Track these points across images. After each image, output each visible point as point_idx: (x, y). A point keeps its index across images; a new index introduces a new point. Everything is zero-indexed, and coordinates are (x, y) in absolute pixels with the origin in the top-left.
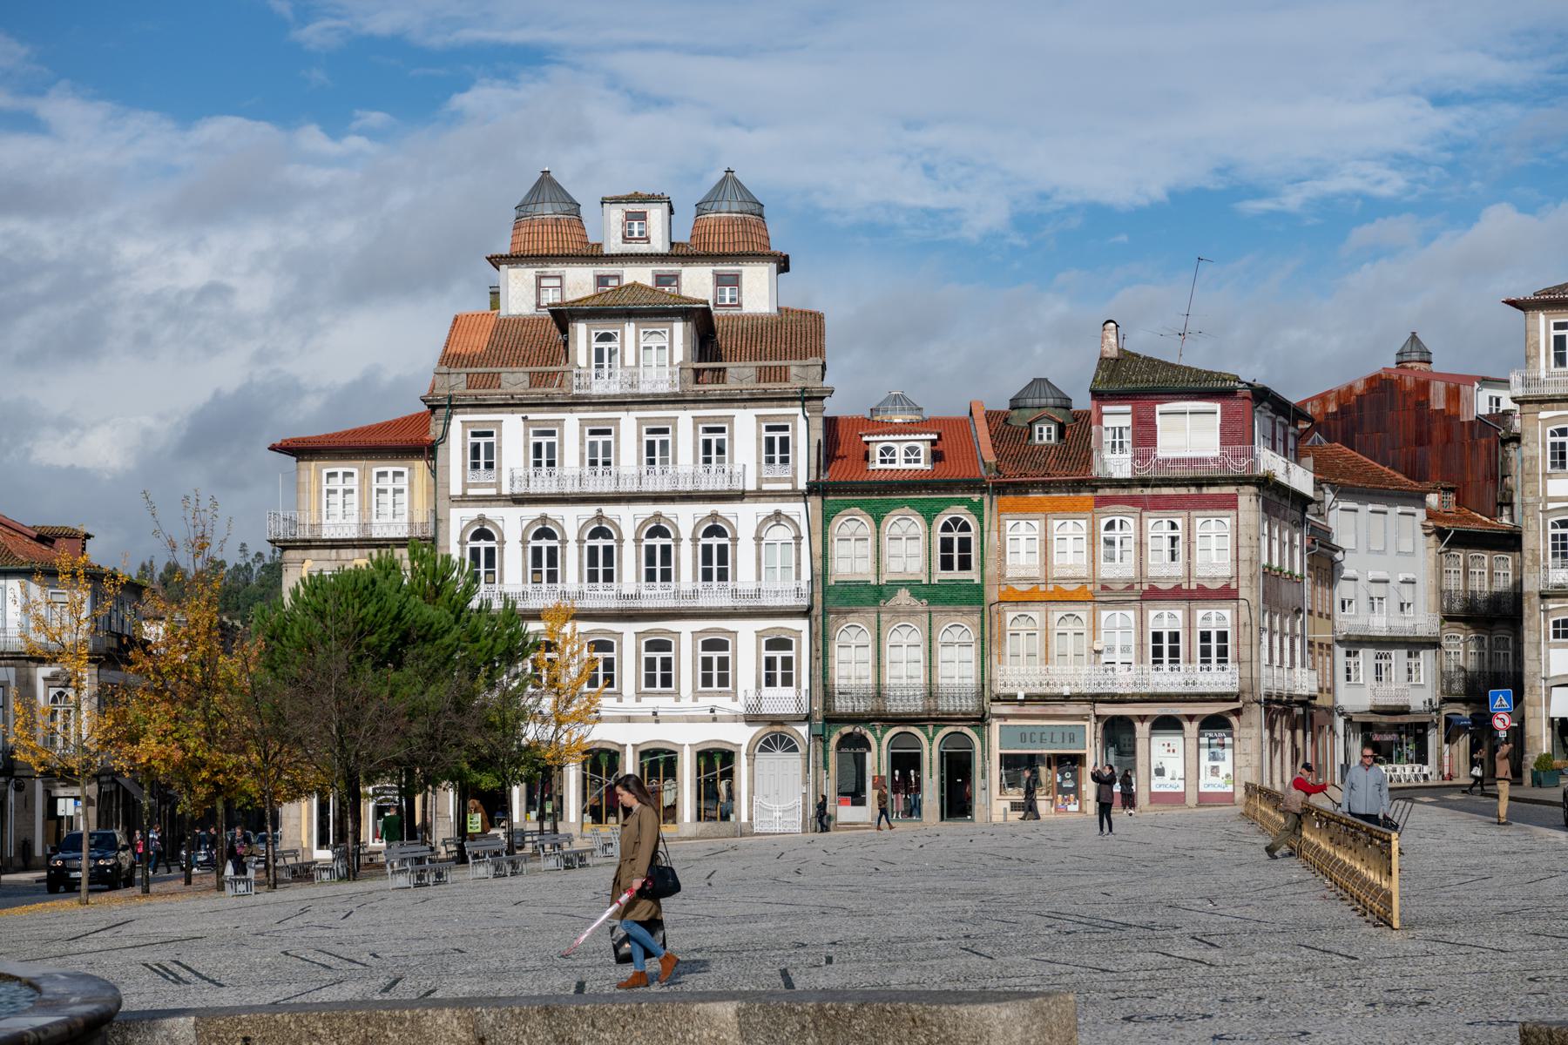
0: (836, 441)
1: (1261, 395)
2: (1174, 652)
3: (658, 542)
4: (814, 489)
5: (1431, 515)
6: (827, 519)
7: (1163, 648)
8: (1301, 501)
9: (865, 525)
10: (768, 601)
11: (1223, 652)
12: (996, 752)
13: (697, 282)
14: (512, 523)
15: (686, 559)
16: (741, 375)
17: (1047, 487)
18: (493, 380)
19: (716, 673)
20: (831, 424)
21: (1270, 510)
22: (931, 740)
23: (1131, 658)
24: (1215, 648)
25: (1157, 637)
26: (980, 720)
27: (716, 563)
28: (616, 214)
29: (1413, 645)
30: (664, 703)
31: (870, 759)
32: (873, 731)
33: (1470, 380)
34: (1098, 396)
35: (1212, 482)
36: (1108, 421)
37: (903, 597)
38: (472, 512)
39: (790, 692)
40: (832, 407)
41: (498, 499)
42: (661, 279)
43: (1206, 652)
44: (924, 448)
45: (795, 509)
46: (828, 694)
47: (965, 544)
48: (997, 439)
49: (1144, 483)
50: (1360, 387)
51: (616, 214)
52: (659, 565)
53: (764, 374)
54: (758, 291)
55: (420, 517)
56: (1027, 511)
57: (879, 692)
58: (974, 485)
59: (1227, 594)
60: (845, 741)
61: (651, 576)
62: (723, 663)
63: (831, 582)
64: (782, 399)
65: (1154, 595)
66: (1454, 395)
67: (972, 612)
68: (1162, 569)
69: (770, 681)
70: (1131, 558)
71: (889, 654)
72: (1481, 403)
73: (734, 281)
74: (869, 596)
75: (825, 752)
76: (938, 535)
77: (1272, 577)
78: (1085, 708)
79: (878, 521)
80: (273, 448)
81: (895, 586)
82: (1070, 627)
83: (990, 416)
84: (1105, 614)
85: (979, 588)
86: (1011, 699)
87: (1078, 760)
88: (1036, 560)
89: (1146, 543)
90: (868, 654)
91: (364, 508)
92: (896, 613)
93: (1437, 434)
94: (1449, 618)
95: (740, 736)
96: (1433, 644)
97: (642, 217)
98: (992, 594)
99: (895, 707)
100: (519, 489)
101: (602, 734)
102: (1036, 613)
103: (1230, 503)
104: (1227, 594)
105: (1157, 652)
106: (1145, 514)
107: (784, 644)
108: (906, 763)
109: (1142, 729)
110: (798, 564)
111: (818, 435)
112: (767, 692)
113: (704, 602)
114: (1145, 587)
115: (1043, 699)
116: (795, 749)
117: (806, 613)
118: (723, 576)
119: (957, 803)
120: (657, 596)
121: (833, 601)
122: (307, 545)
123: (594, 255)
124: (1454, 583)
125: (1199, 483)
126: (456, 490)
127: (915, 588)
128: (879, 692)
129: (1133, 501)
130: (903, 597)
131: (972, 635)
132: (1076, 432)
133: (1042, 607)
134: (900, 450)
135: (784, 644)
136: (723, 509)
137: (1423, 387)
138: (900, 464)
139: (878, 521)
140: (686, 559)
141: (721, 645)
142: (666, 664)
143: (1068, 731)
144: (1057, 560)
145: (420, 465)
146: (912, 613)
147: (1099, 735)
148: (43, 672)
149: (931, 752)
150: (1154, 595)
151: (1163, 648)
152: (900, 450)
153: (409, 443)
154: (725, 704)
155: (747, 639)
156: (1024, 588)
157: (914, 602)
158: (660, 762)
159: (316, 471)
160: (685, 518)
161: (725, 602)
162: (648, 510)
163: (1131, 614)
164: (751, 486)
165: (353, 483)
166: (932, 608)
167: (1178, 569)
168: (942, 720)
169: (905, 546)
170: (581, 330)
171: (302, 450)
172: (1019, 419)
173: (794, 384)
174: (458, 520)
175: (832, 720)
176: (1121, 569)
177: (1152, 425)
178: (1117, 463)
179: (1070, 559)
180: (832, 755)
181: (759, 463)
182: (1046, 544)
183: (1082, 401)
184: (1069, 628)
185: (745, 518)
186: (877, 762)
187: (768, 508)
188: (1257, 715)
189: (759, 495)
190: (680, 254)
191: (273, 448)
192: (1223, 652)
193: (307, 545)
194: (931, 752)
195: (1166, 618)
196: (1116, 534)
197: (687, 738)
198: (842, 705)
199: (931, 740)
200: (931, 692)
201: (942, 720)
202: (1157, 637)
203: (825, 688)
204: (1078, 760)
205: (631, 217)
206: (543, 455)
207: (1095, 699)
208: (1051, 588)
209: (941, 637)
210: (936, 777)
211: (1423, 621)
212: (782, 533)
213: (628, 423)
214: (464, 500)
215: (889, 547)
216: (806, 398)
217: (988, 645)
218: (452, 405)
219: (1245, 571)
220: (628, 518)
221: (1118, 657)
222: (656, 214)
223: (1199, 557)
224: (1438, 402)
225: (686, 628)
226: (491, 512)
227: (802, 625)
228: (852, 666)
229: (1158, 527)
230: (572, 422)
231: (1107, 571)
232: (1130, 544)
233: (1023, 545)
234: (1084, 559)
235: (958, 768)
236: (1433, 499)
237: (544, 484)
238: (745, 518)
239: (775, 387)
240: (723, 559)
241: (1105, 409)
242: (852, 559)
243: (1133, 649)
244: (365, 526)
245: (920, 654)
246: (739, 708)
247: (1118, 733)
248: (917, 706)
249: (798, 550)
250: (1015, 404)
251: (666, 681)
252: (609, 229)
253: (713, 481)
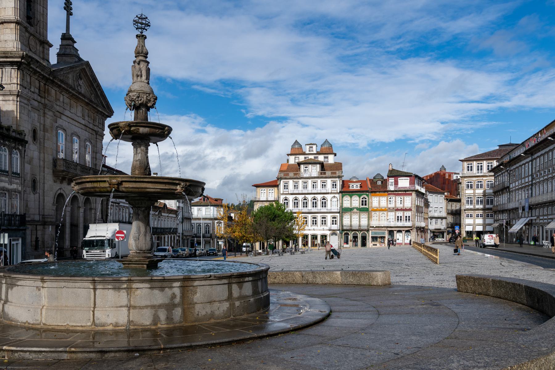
0: (344, 184)
1: (416, 176)
2: (401, 219)
3: (315, 201)
4: (340, 192)
5: (445, 196)
6: (342, 197)
7: (399, 219)
8: (423, 194)
9: (349, 198)
10: (332, 211)
11: (409, 219)
12: (370, 236)
13: (321, 158)
14: (291, 198)
15: (319, 203)
16: (328, 173)
17: (379, 192)
18: (288, 175)
19: (324, 222)
20: (343, 181)
21: (417, 196)
24: (408, 219)
25: (398, 217)
26: (368, 231)
27: (324, 204)
28: (308, 147)
29: (442, 218)
30: (315, 227)
31: (349, 237)
33: (452, 173)
34: (388, 176)
35: (408, 191)
36: (390, 181)
37: (355, 210)
38: (284, 196)
39: (336, 226)
40: (343, 179)
41: (288, 194)
42: (315, 158)
43: (406, 219)
44: (359, 185)
45: (337, 195)
46: (342, 226)
47: (366, 201)
48: (371, 184)
49: (396, 191)
50: (433, 175)
51: (308, 147)
52: (315, 205)
53: (332, 173)
54: (331, 159)
55: (276, 197)
56: (376, 196)
57: (351, 226)
58: (367, 191)
59: (410, 210)
60: (345, 234)
61: (313, 206)
62: (325, 221)
64: (335, 177)
65: (397, 210)
66: (450, 176)
68: (399, 206)
69: (333, 224)
70: (394, 204)
71: (353, 220)
72: (455, 177)
73: (327, 158)
74: (349, 210)
76: (361, 200)
77: (418, 207)
78: (385, 229)
79: (351, 197)
81: (354, 208)
82: (383, 215)
83: (370, 180)
85: (368, 209)
86: (373, 227)
87: (384, 237)
88: (378, 204)
89: (397, 201)
90: (349, 219)
91: (267, 195)
92: (354, 213)
93: (447, 183)
94: (448, 214)
95: (328, 233)
96: (446, 218)
97: (312, 147)
98: (370, 210)
99: (353, 228)
100: (292, 192)
101: (306, 232)
102: (377, 213)
103: (411, 194)
104: (410, 210)
105: (398, 219)
107: (335, 218)
108: (355, 237)
109: (395, 232)
111: (341, 183)
112: (332, 226)
113: (322, 211)
115: (378, 227)
117: (339, 213)
118: (325, 206)
119: (364, 244)
120: (314, 210)
121: (344, 211)
122: (258, 201)
123: (304, 154)
124: (449, 208)
125: (405, 191)
126: (282, 192)
127: (357, 209)
128: (351, 226)
130: (355, 210)
131: (367, 216)
132: (385, 183)
134: (355, 186)
135: (335, 218)
136: (325, 195)
137: (444, 174)
138: (355, 188)
139: (351, 197)
140: (319, 203)
141: (325, 218)
142: (316, 221)
144: (381, 204)
145: (276, 188)
146: (357, 213)
148: (216, 221)
149: (359, 235)
150: (397, 210)
151: (399, 219)
152: (355, 186)
153: (274, 185)
154: (325, 228)
155: (329, 217)
158: (314, 237)
159: (259, 189)
160: (319, 197)
161: (326, 211)
162: (313, 196)
163: (394, 213)
164: (330, 192)
165: (265, 191)
167: (402, 206)
168: (361, 230)
169: (356, 202)
170: (302, 166)
171: (257, 186)
172: (375, 180)
173: (337, 175)
174: (282, 197)
175: (343, 230)
176: (392, 206)
177: (398, 181)
178: (391, 188)
179: (383, 204)
182: (379, 201)
183: (385, 177)
184: (383, 215)
185: (329, 197)
186: (350, 237)
187: (333, 195)
188: (415, 230)
189: (331, 193)
190: (318, 153)
192: (409, 219)
193: (258, 201)
194: (359, 235)
195: (400, 214)
196: (391, 200)
197: (319, 233)
198: (345, 228)
200: (360, 226)
201: (361, 230)
202: (398, 217)
204: (384, 237)
205: (310, 147)
206: (296, 187)
207: (387, 227)
209: (361, 217)
211: (444, 214)
212: (335, 199)
213: (310, 181)
214: (283, 194)
215: (353, 202)
216: (339, 177)
217: (369, 218)
218: (281, 179)
219: (413, 206)
220: (310, 197)
221: (391, 220)
222: (314, 147)
223: (405, 204)
224: (447, 177)
225: (319, 215)
226: (287, 196)
227: (338, 215)
228: (346, 221)
229: (398, 198)
230: (300, 181)
231: (390, 206)
232: (394, 201)
234: (386, 204)
235: (364, 239)
236: (446, 194)
237: (296, 191)
238: (329, 197)
239: (334, 175)
240: (325, 204)
242: (347, 203)
244: (267, 198)
245: (358, 219)
246: (328, 228)
247: (391, 233)
248: (357, 228)
250: (374, 178)
251: (316, 224)
252: (307, 149)
253: (324, 191)
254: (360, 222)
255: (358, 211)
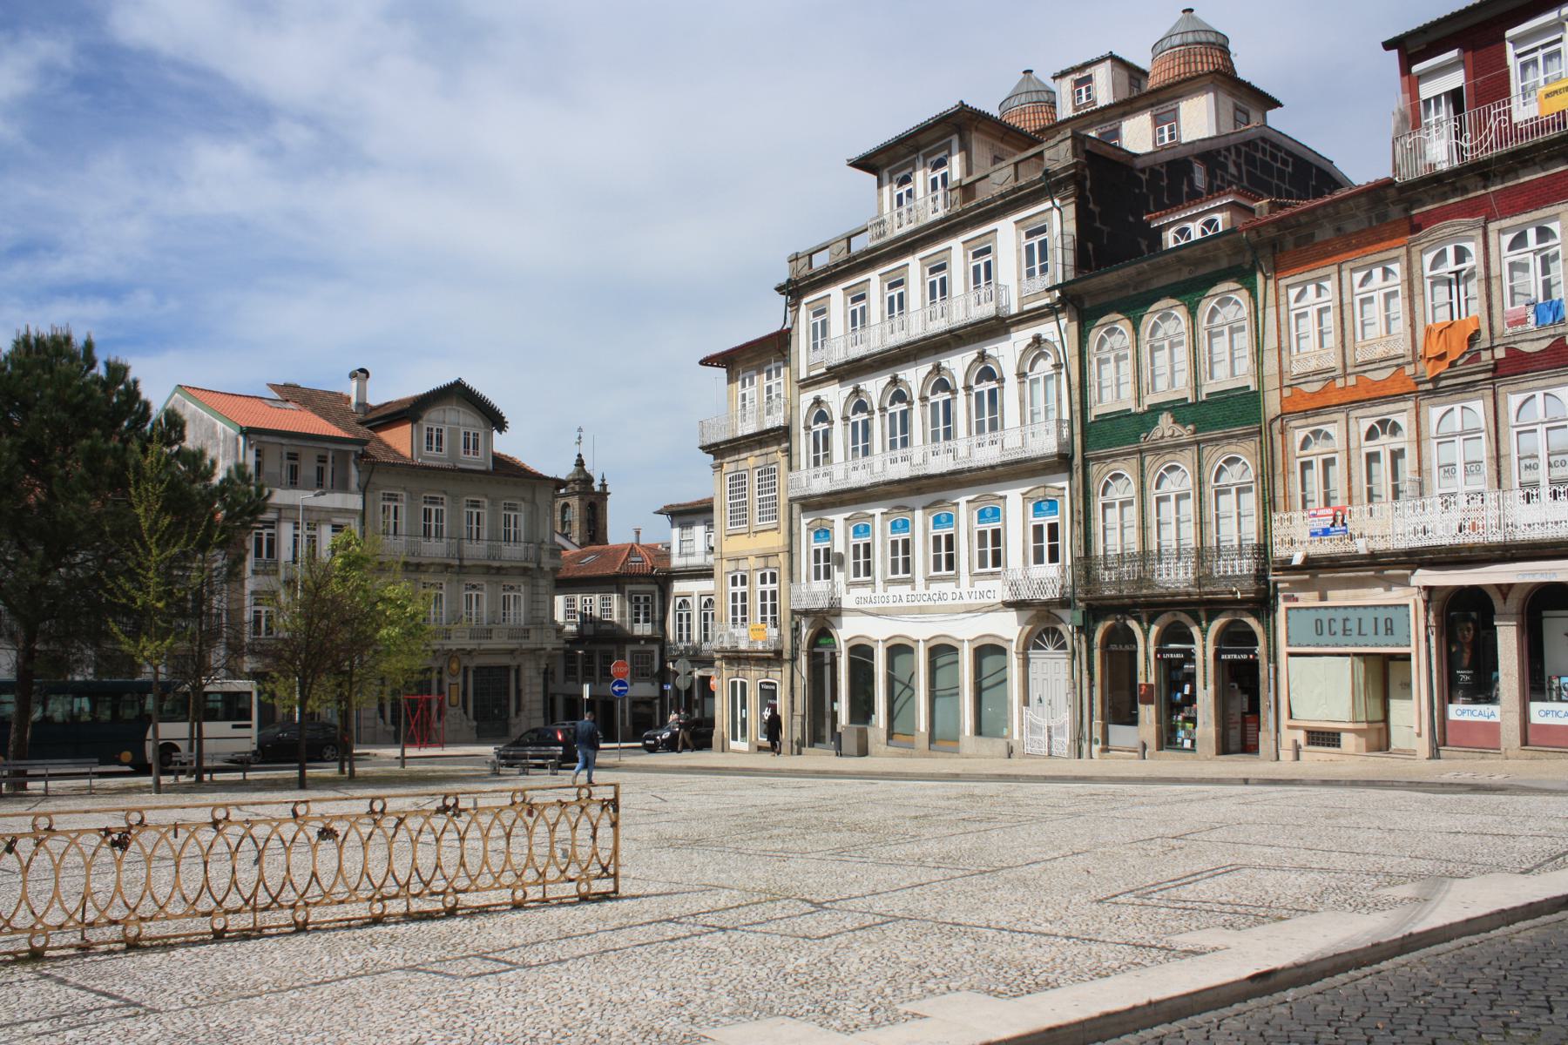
22: (1204, 632)
23: (1482, 481)
26: (1263, 604)
32: (1140, 623)
45: (1048, 329)
63: (1091, 418)
67: (1247, 436)
75: (1090, 650)
80: (701, 363)
81: (1156, 410)
82: (1384, 444)
84: (1434, 413)
92: (1157, 450)
98: (1272, 404)
106: (1493, 227)
110: (1059, 400)
114: (1500, 353)
116: (1063, 646)
126: (803, 375)
129: (1469, 210)
133: (1341, 417)
143: (1382, 615)
147: (1432, 621)
156: (1316, 387)
157: (1178, 430)
163: (1478, 408)
166: (1199, 436)
180: (1097, 653)
181: (1019, 280)
187: (1021, 337)
191: (701, 363)
197: (966, 631)
199: (1204, 632)
203: (1086, 562)
208: (1352, 381)
210: (1211, 688)
233: (1309, 325)
238: (1007, 352)
241: (1416, 68)
243: (1485, 467)
249: (1059, 381)
254: (1201, 524)
255: (1185, 433)
